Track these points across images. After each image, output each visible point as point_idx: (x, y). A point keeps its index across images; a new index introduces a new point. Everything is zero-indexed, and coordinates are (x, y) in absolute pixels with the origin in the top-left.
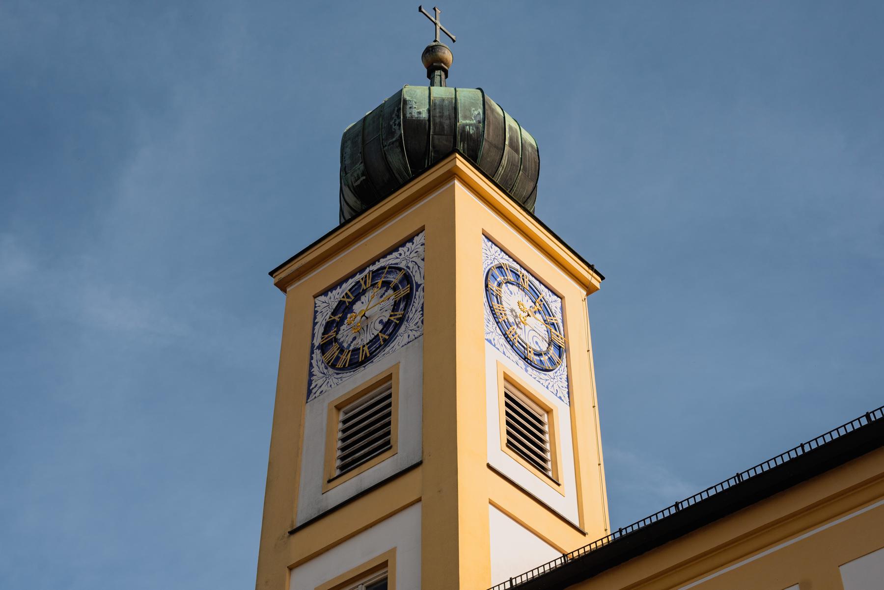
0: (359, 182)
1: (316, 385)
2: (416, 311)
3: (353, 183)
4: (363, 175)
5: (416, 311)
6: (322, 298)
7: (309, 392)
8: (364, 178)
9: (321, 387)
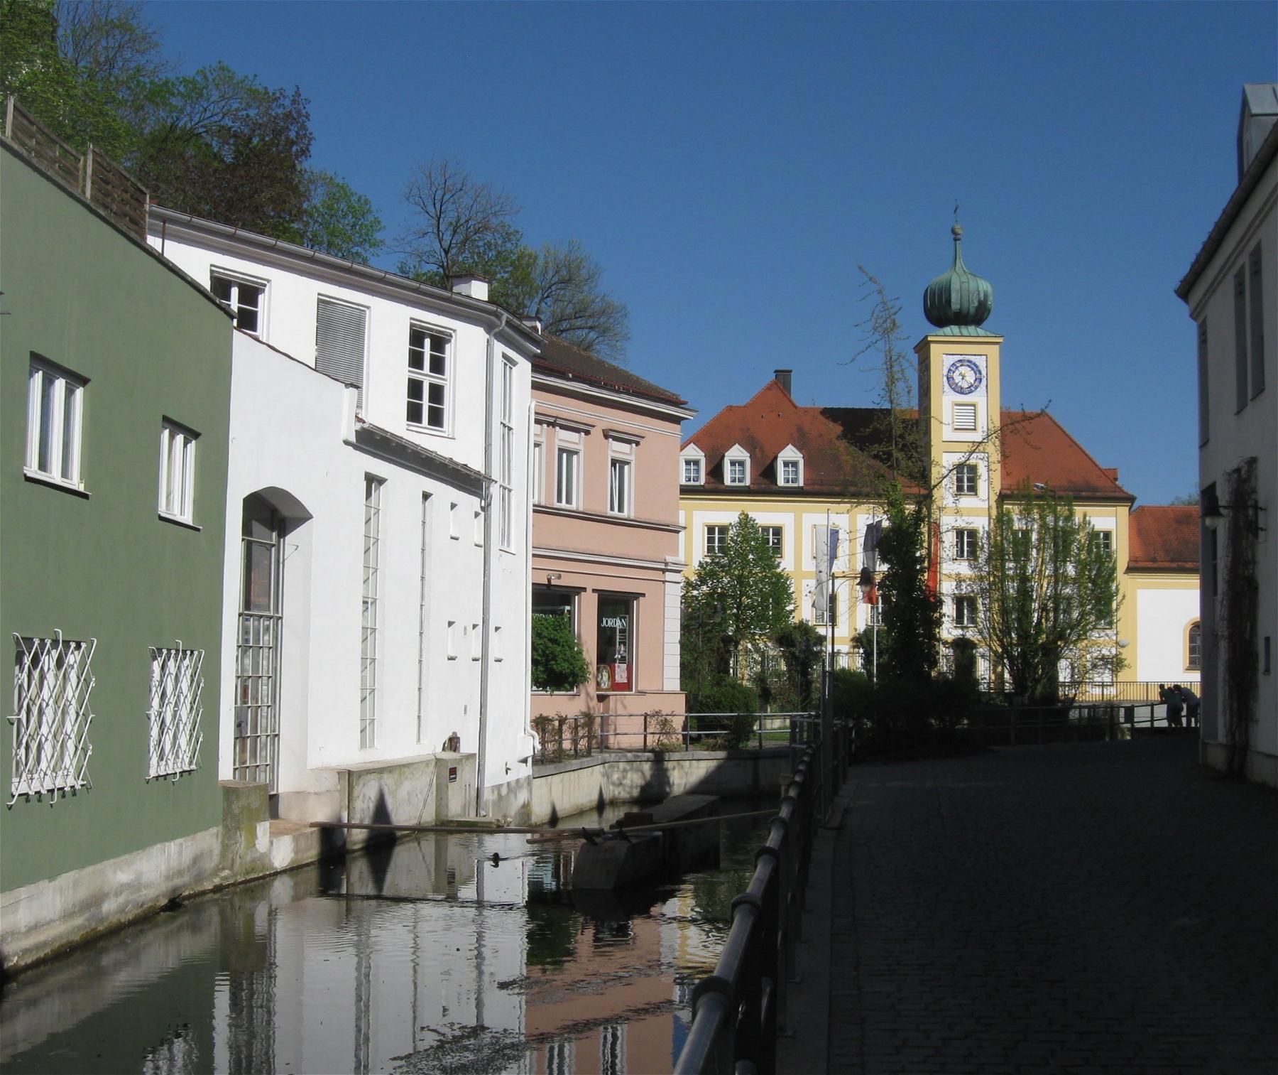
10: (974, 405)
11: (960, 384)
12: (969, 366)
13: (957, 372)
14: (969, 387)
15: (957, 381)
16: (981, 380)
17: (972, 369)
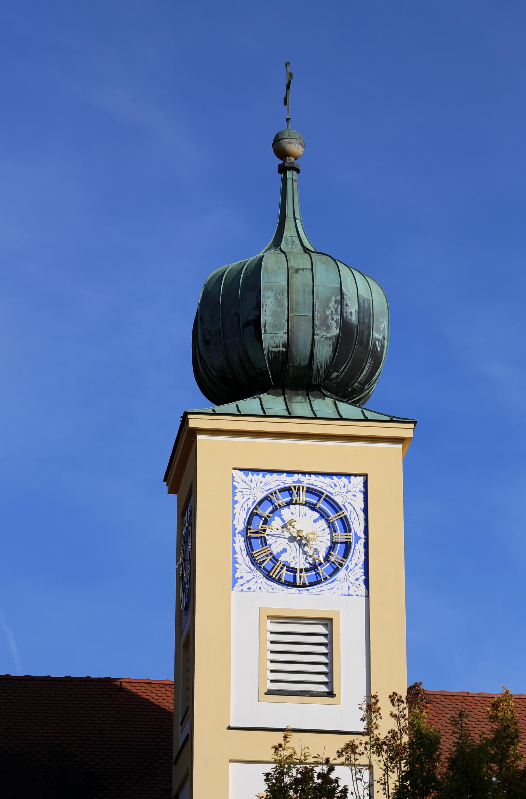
0: (276, 350)
1: (242, 577)
2: (356, 565)
3: (270, 347)
5: (356, 565)
6: (241, 473)
7: (235, 581)
8: (284, 350)
9: (248, 581)
10: (328, 622)
11: (282, 558)
12: (313, 507)
13: (277, 523)
14: (314, 567)
15: (275, 549)
16: (348, 546)
17: (323, 515)
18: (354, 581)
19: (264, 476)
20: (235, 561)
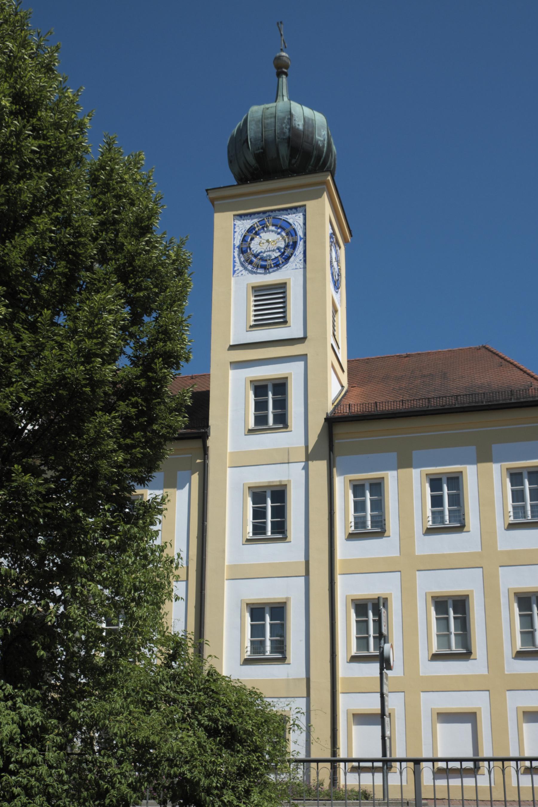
0: (258, 152)
1: (238, 269)
4: (262, 148)
8: (262, 151)
18: (299, 261)
19: (250, 216)
20: (234, 262)
